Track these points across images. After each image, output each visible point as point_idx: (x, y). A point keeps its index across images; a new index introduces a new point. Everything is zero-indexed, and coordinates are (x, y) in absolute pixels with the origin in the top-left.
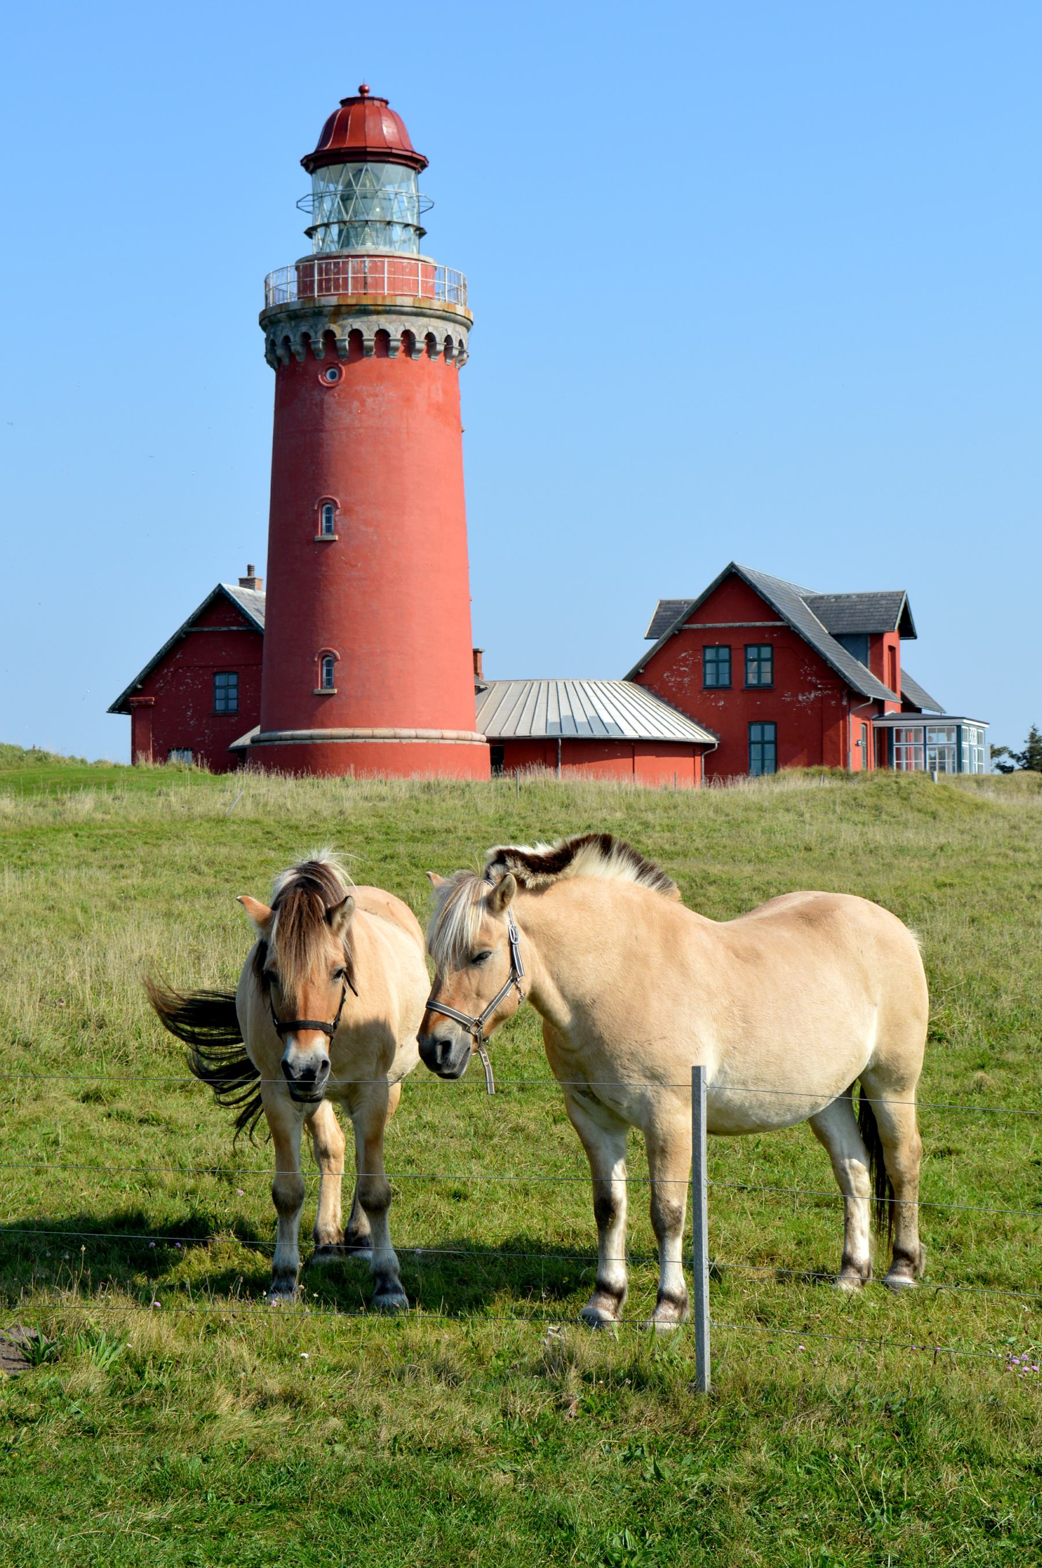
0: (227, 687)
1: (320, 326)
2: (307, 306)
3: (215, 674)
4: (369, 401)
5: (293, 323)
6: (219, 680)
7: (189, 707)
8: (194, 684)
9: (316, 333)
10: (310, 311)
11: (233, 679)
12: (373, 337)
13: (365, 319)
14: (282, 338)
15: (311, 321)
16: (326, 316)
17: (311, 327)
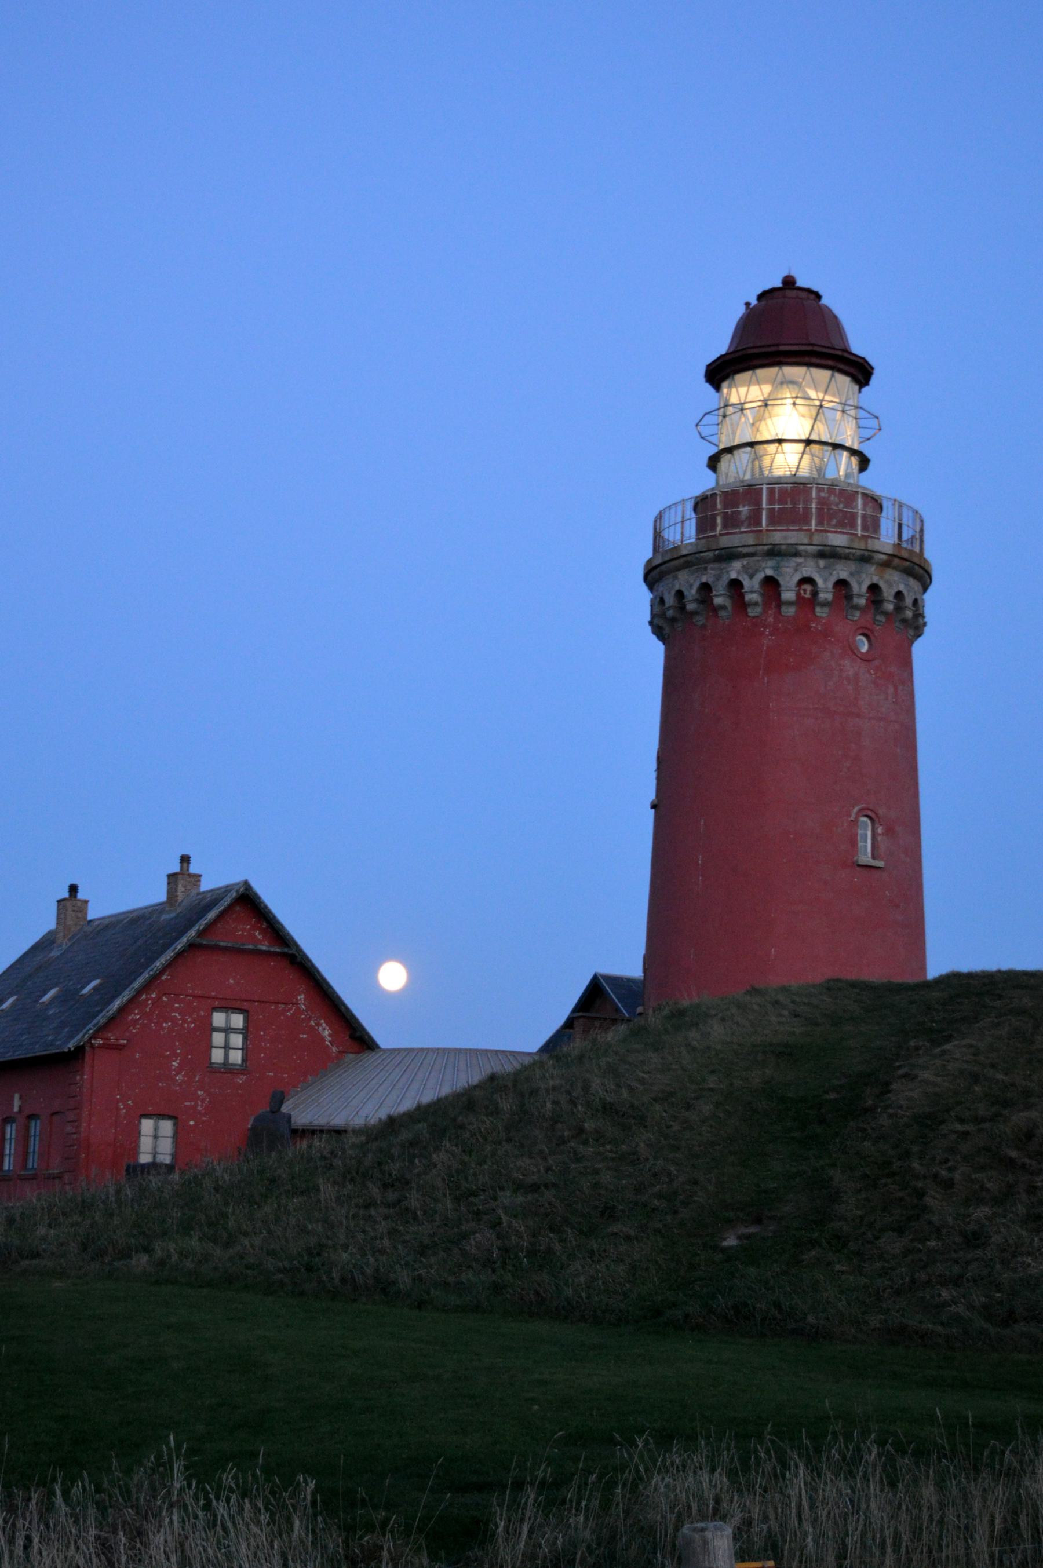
0: (227, 1030)
1: (864, 576)
2: (856, 545)
3: (216, 1009)
4: (900, 687)
5: (822, 563)
6: (219, 1019)
7: (177, 1056)
8: (184, 1021)
9: (860, 584)
10: (859, 553)
11: (238, 1020)
12: (911, 606)
13: (905, 576)
14: (797, 578)
15: (852, 566)
16: (873, 564)
17: (852, 574)
